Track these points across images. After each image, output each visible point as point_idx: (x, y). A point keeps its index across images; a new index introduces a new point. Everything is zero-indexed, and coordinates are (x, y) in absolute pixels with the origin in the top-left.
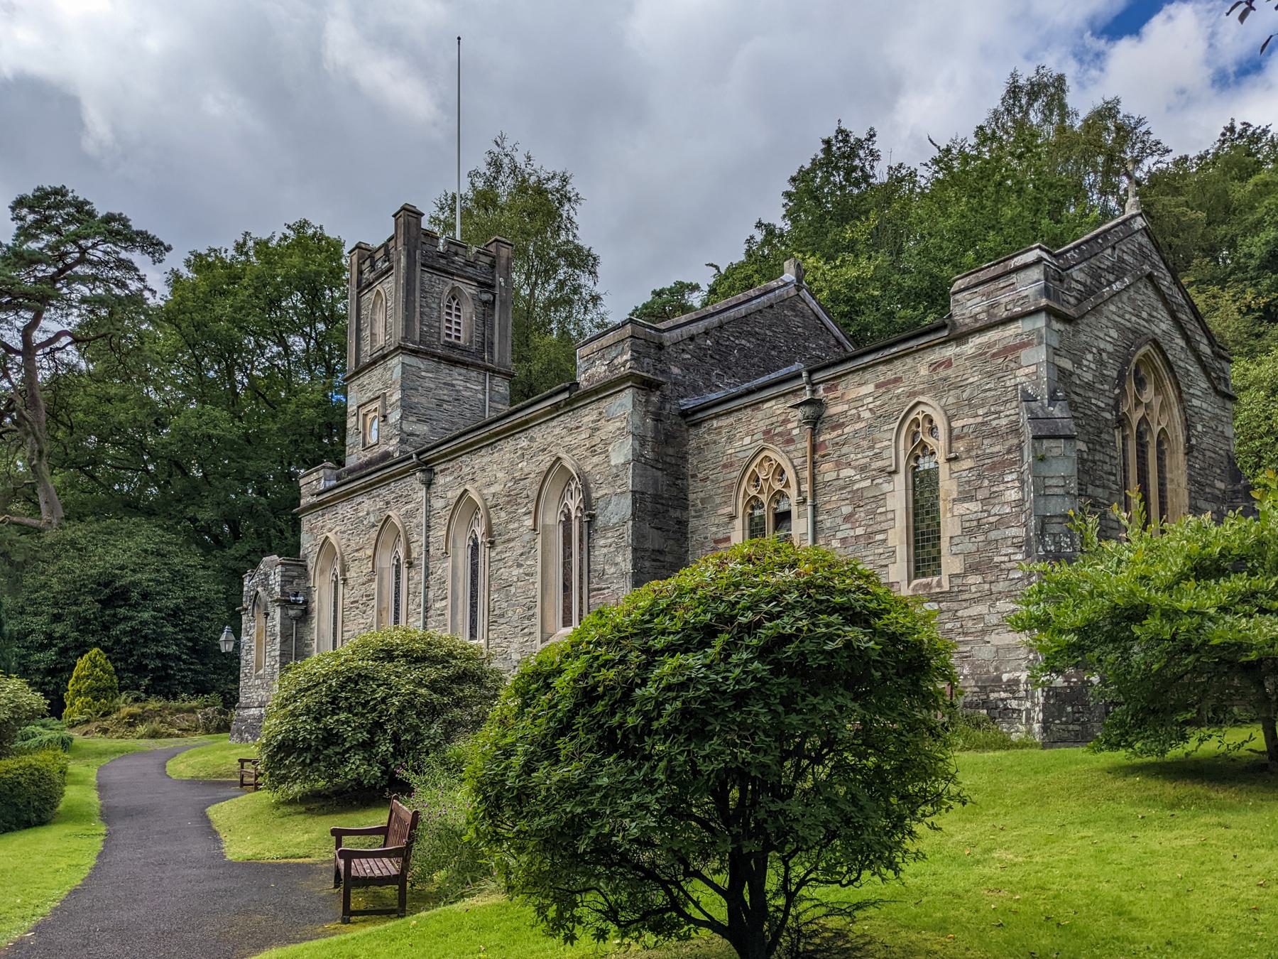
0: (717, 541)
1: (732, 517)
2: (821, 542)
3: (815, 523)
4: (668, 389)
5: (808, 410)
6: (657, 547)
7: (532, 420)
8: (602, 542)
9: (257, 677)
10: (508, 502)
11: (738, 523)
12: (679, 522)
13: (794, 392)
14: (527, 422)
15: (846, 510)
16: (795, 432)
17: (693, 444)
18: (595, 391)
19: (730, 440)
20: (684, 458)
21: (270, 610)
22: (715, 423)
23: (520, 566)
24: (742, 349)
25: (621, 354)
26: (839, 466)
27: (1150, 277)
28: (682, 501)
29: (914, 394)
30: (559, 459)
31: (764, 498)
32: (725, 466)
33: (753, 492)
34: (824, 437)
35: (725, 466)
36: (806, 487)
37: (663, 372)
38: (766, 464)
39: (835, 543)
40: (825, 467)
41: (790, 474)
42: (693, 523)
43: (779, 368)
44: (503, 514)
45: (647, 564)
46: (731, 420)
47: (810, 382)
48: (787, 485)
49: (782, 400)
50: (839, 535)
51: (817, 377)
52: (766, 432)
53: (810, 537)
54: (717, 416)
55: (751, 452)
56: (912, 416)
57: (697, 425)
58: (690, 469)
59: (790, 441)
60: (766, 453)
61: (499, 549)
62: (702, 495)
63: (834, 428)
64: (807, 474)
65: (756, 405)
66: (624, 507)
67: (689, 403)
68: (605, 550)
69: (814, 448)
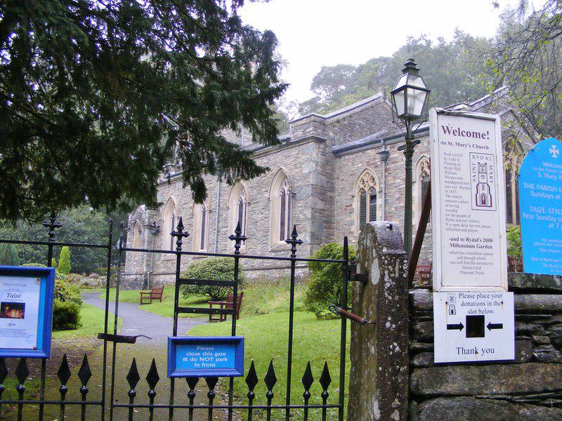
0: (347, 206)
1: (353, 197)
2: (388, 208)
3: (385, 200)
4: (328, 142)
5: (384, 156)
6: (322, 208)
7: (268, 152)
8: (299, 205)
9: (135, 261)
10: (257, 186)
11: (355, 199)
12: (331, 197)
13: (378, 147)
14: (266, 152)
15: (397, 196)
16: (379, 163)
17: (338, 165)
18: (297, 142)
19: (353, 164)
20: (333, 170)
21: (142, 230)
22: (347, 157)
23: (262, 214)
24: (360, 124)
25: (309, 128)
26: (395, 178)
27: (511, 111)
28: (332, 189)
29: (421, 153)
30: (281, 169)
31: (366, 189)
32: (351, 175)
33: (362, 186)
34: (390, 166)
35: (351, 175)
36: (382, 186)
37: (325, 135)
38: (367, 175)
39: (393, 209)
40: (389, 178)
41: (377, 180)
42: (337, 198)
43: (375, 132)
44: (255, 191)
45: (317, 214)
46: (354, 156)
47: (384, 144)
48: (375, 184)
49: (374, 150)
50: (395, 206)
51: (388, 142)
52: (367, 163)
53: (383, 206)
54: (348, 154)
55: (361, 170)
56: (421, 161)
57: (340, 157)
58: (336, 176)
59: (377, 167)
60: (366, 171)
61: (252, 206)
62: (341, 187)
63: (393, 163)
64: (383, 181)
65: (363, 151)
66: (309, 190)
67: (336, 148)
68: (300, 209)
69: (386, 170)
